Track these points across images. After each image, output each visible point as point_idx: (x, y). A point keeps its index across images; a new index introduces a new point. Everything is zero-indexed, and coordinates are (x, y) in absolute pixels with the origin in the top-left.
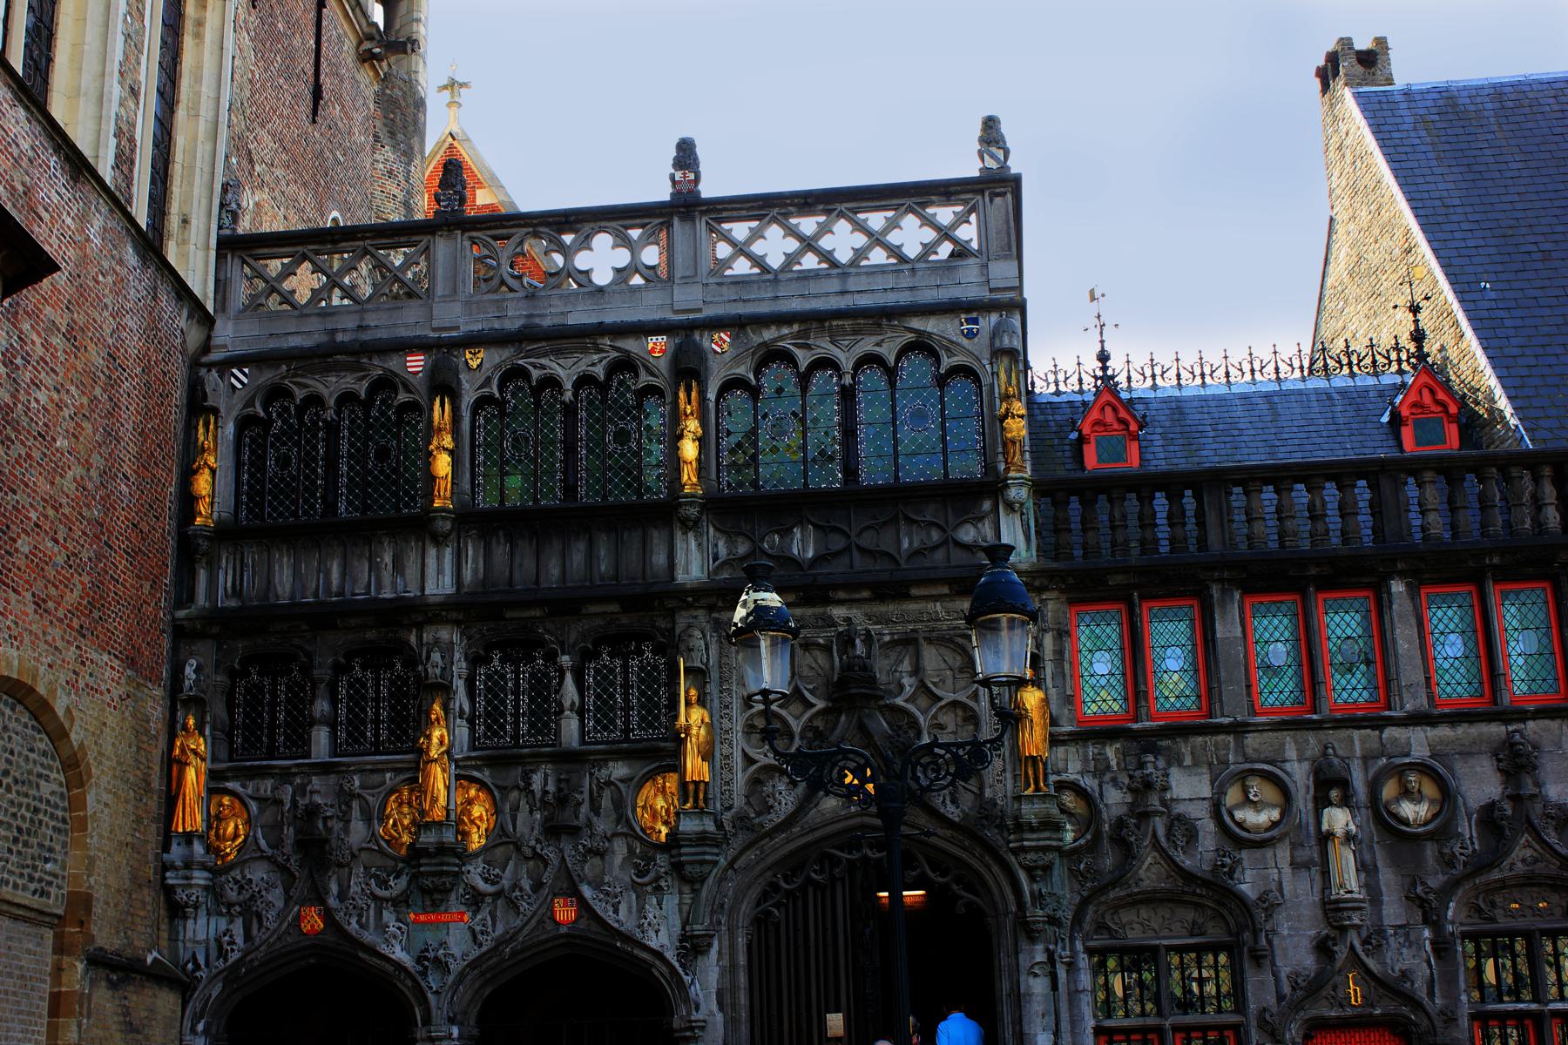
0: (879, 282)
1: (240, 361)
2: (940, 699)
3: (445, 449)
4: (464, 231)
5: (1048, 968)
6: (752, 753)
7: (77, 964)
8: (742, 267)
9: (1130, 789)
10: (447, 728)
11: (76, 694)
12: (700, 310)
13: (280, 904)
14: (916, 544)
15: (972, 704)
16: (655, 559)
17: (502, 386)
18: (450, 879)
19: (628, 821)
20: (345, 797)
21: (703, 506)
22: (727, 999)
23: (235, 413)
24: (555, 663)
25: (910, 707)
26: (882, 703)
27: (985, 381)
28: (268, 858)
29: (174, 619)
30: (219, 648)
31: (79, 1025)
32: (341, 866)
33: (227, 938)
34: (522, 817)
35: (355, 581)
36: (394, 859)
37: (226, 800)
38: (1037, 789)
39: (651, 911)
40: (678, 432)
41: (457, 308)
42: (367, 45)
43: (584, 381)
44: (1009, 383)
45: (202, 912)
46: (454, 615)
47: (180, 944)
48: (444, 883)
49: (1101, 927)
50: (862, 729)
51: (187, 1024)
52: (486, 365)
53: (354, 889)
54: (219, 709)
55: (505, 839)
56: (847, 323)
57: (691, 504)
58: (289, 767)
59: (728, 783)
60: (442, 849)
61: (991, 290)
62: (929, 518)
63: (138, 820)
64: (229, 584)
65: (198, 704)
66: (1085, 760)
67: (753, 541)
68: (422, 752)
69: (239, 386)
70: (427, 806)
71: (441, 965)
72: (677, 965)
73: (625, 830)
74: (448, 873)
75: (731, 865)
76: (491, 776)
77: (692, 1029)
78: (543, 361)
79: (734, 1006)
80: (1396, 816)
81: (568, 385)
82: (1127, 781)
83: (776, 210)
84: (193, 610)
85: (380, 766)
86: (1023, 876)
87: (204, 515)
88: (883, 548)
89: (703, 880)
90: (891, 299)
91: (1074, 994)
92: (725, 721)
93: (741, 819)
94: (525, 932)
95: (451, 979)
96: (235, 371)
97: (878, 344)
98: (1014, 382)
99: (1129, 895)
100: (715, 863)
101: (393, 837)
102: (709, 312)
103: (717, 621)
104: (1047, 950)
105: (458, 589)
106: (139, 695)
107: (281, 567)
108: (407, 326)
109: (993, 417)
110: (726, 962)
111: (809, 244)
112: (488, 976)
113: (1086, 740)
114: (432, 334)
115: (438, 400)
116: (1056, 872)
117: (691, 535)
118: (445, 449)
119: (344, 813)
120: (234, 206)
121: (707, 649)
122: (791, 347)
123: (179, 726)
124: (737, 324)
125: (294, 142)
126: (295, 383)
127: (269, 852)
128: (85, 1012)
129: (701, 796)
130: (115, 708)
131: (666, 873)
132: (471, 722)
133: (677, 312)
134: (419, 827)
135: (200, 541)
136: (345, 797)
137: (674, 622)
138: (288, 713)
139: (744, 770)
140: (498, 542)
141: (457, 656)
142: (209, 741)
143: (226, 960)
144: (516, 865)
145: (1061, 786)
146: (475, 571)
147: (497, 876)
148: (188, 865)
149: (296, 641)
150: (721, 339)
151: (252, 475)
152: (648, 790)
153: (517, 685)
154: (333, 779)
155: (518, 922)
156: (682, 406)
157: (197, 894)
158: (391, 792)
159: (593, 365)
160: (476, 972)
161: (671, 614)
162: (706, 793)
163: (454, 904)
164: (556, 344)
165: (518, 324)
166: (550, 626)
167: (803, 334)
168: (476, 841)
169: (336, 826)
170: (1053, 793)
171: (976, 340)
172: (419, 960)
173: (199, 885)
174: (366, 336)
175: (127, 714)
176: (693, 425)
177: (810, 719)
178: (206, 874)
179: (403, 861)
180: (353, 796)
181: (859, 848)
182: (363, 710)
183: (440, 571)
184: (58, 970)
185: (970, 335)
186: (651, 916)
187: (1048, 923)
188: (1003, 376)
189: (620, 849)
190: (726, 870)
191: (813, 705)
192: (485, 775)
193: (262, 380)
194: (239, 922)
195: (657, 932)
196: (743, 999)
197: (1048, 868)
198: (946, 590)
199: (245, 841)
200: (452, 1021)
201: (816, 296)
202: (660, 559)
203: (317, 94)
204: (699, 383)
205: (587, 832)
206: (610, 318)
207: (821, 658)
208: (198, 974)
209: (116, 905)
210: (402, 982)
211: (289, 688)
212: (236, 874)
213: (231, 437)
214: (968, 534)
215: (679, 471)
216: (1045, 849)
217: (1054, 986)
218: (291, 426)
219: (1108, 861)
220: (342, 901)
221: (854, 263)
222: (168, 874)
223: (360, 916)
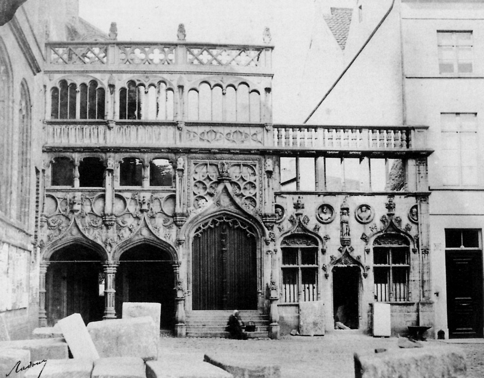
2: (246, 181)
6: (196, 192)
15: (254, 182)
28: (63, 215)
33: (51, 236)
50: (225, 188)
77: (178, 264)
80: (359, 217)
89: (182, 225)
100: (185, 221)
127: (62, 213)
181: (223, 219)
187: (271, 241)
197: (272, 227)
205: (150, 211)
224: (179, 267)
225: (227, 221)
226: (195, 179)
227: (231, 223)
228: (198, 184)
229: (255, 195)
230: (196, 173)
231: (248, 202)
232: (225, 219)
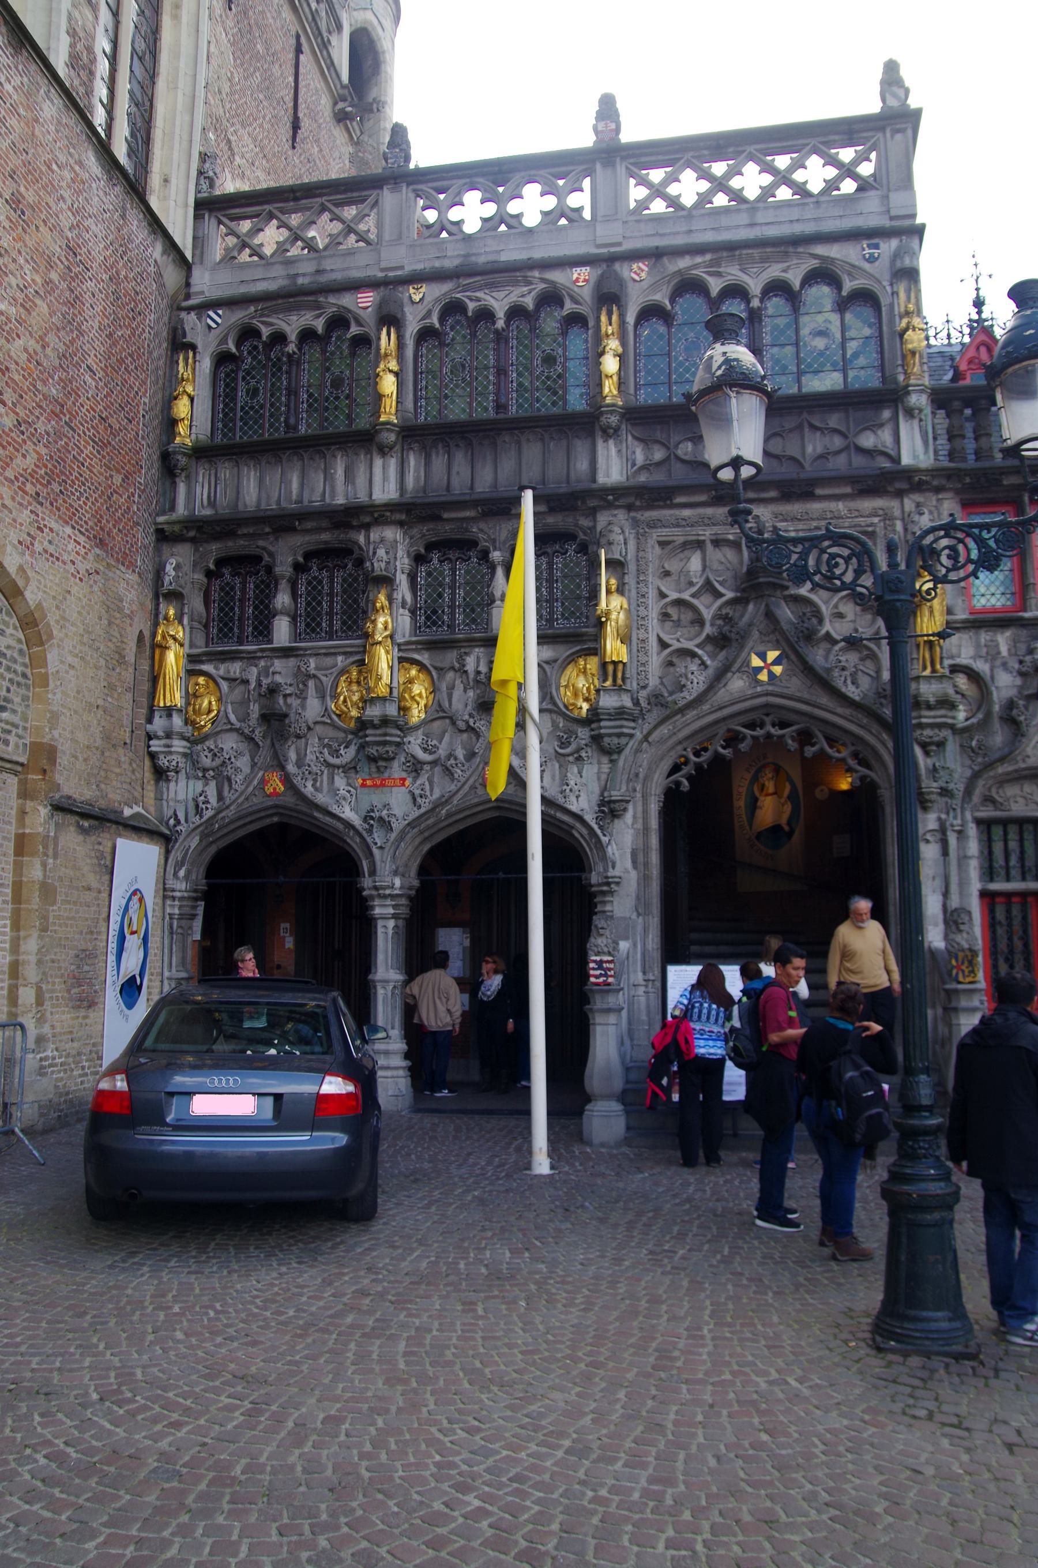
0: (786, 215)
1: (214, 304)
3: (391, 371)
4: (409, 184)
5: (939, 836)
6: (666, 638)
7: (40, 808)
8: (658, 206)
9: (1022, 674)
10: (391, 614)
11: (32, 556)
12: (619, 244)
13: (247, 770)
14: (819, 450)
16: (578, 465)
17: (442, 319)
18: (393, 748)
19: (552, 698)
20: (303, 677)
21: (623, 416)
22: (641, 859)
23: (211, 349)
24: (487, 561)
26: (786, 593)
27: (884, 301)
28: (237, 730)
29: (156, 524)
30: (196, 550)
31: (44, 865)
32: (298, 737)
33: (202, 798)
35: (313, 490)
36: (345, 731)
37: (201, 680)
38: (934, 671)
39: (573, 779)
40: (600, 349)
41: (402, 251)
42: (341, 105)
43: (516, 312)
44: (909, 300)
45: (182, 776)
47: (165, 803)
49: (988, 800)
50: (769, 615)
51: (170, 870)
52: (428, 299)
53: (310, 757)
54: (196, 603)
55: (442, 714)
56: (756, 252)
57: (612, 412)
58: (255, 652)
59: (643, 665)
60: (385, 721)
61: (892, 218)
63: (111, 687)
64: (205, 496)
65: (175, 596)
66: (978, 646)
67: (668, 448)
68: (367, 636)
69: (214, 325)
70: (372, 684)
71: (385, 824)
72: (596, 827)
73: (550, 706)
74: (390, 743)
75: (646, 738)
76: (430, 659)
77: (608, 884)
78: (479, 294)
79: (646, 864)
81: (500, 314)
82: (1017, 666)
83: (691, 154)
84: (174, 517)
87: (184, 436)
88: (789, 453)
89: (620, 750)
90: (798, 229)
91: (963, 859)
92: (641, 609)
93: (656, 696)
94: (459, 796)
95: (393, 836)
96: (211, 313)
97: (785, 271)
98: (913, 300)
99: (1016, 771)
100: (631, 736)
101: (343, 712)
102: (628, 246)
103: (634, 519)
104: (939, 819)
105: (401, 495)
106: (111, 574)
107: (249, 480)
108: (358, 268)
109: (893, 332)
110: (639, 825)
111: (720, 184)
112: (426, 834)
113: (979, 627)
117: (611, 442)
118: (391, 371)
119: (302, 691)
120: (211, 174)
123: (161, 616)
124: (655, 255)
125: (274, 155)
126: (263, 323)
127: (238, 725)
128: (51, 852)
129: (620, 675)
130: (81, 580)
132: (413, 612)
133: (599, 246)
134: (365, 702)
135: (179, 457)
136: (303, 677)
137: (595, 520)
138: (256, 608)
139: (658, 654)
140: (437, 453)
141: (400, 554)
142: (187, 629)
143: (201, 817)
144: (451, 737)
145: (955, 669)
146: (417, 479)
147: (435, 746)
148: (169, 735)
149: (261, 543)
151: (226, 405)
152: (571, 672)
153: (454, 580)
154: (292, 662)
155: (453, 787)
156: (603, 330)
157: (176, 759)
158: (343, 671)
159: (523, 296)
160: (415, 830)
161: (593, 512)
162: (623, 673)
163: (396, 770)
164: (489, 278)
165: (456, 262)
166: (482, 525)
167: (715, 263)
168: (417, 714)
169: (294, 702)
170: (947, 672)
171: (877, 263)
172: (366, 819)
173: (178, 753)
174: (323, 279)
175: (96, 588)
176: (613, 344)
177: (720, 608)
178: (185, 743)
179: (352, 733)
180: (310, 676)
181: (762, 726)
182: (320, 603)
183: (385, 479)
184: (22, 813)
185: (872, 259)
186: (572, 783)
187: (941, 794)
188: (902, 295)
190: (641, 742)
191: (722, 595)
192: (424, 657)
193: (233, 320)
194: (213, 784)
195: (577, 797)
196: (655, 858)
197: (941, 744)
198: (848, 490)
199: (217, 715)
200: (396, 873)
201: (728, 228)
202: (582, 465)
203: (296, 126)
204: (619, 308)
206: (538, 254)
207: (730, 554)
208: (178, 828)
209: (85, 760)
210: (351, 838)
211: (257, 587)
212: (210, 743)
214: (867, 440)
215: (600, 385)
216: (940, 726)
217: (945, 853)
218: (260, 362)
219: (998, 737)
220: (299, 767)
221: (761, 199)
222: (151, 743)
223: (315, 780)
224: (611, 893)
225: (781, 732)
226: (662, 595)
227: (793, 739)
228: (673, 611)
230: (667, 574)
231: (851, 658)
232: (773, 725)
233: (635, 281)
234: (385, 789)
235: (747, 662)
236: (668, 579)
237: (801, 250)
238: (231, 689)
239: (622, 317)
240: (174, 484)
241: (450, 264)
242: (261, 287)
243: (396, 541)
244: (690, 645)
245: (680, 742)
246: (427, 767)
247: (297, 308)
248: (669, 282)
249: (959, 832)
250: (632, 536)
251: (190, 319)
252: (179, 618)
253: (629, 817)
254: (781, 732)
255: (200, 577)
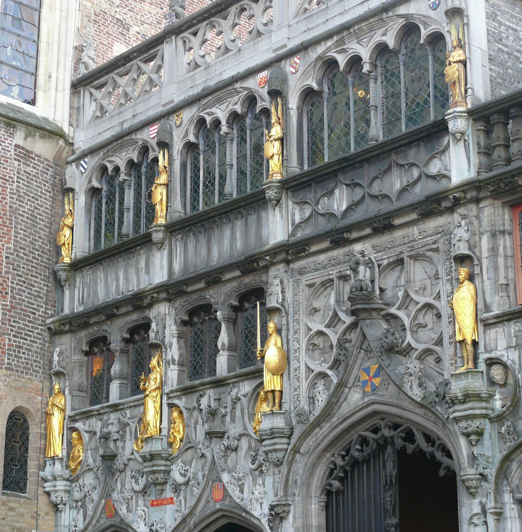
1: (84, 155)
12: (285, 46)
14: (405, 183)
15: (435, 303)
18: (162, 475)
23: (84, 188)
25: (401, 314)
26: (383, 313)
32: (121, 472)
34: (199, 427)
45: (68, 506)
46: (163, 295)
47: (59, 528)
48: (157, 479)
52: (185, 121)
53: (127, 486)
62: (411, 161)
74: (159, 471)
85: (137, 403)
86: (463, 442)
96: (82, 162)
97: (384, 34)
104: (481, 503)
108: (152, 108)
113: (509, 320)
114: (164, 109)
115: (161, 152)
116: (486, 435)
121: (283, 292)
122: (335, 55)
126: (110, 162)
131: (264, 460)
135: (61, 273)
142: (69, 398)
145: (491, 362)
150: (295, 62)
154: (118, 415)
166: (211, 292)
167: (341, 42)
170: (482, 367)
173: (62, 490)
178: (65, 483)
189: (244, 443)
191: (345, 323)
192: (181, 403)
194: (81, 511)
197: (480, 434)
198: (414, 216)
202: (264, 233)
212: (81, 481)
213: (84, 204)
214: (435, 168)
222: (46, 485)
223: (128, 504)
226: (310, 329)
229: (439, 342)
230: (316, 310)
232: (390, 428)
233: (293, 73)
234: (163, 507)
235: (357, 379)
236: (318, 314)
237: (390, 14)
238: (90, 439)
239: (285, 105)
240: (63, 291)
241: (197, 90)
242: (108, 135)
243: (165, 314)
244: (324, 368)
245: (326, 450)
246: (183, 488)
247: (121, 148)
248: (314, 67)
249: (496, 514)
250: (291, 284)
251: (71, 170)
252: (62, 392)
253: (291, 516)
254: (393, 433)
255: (77, 357)
